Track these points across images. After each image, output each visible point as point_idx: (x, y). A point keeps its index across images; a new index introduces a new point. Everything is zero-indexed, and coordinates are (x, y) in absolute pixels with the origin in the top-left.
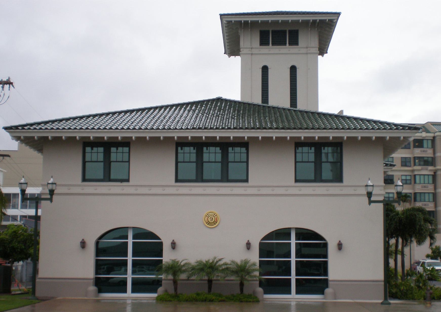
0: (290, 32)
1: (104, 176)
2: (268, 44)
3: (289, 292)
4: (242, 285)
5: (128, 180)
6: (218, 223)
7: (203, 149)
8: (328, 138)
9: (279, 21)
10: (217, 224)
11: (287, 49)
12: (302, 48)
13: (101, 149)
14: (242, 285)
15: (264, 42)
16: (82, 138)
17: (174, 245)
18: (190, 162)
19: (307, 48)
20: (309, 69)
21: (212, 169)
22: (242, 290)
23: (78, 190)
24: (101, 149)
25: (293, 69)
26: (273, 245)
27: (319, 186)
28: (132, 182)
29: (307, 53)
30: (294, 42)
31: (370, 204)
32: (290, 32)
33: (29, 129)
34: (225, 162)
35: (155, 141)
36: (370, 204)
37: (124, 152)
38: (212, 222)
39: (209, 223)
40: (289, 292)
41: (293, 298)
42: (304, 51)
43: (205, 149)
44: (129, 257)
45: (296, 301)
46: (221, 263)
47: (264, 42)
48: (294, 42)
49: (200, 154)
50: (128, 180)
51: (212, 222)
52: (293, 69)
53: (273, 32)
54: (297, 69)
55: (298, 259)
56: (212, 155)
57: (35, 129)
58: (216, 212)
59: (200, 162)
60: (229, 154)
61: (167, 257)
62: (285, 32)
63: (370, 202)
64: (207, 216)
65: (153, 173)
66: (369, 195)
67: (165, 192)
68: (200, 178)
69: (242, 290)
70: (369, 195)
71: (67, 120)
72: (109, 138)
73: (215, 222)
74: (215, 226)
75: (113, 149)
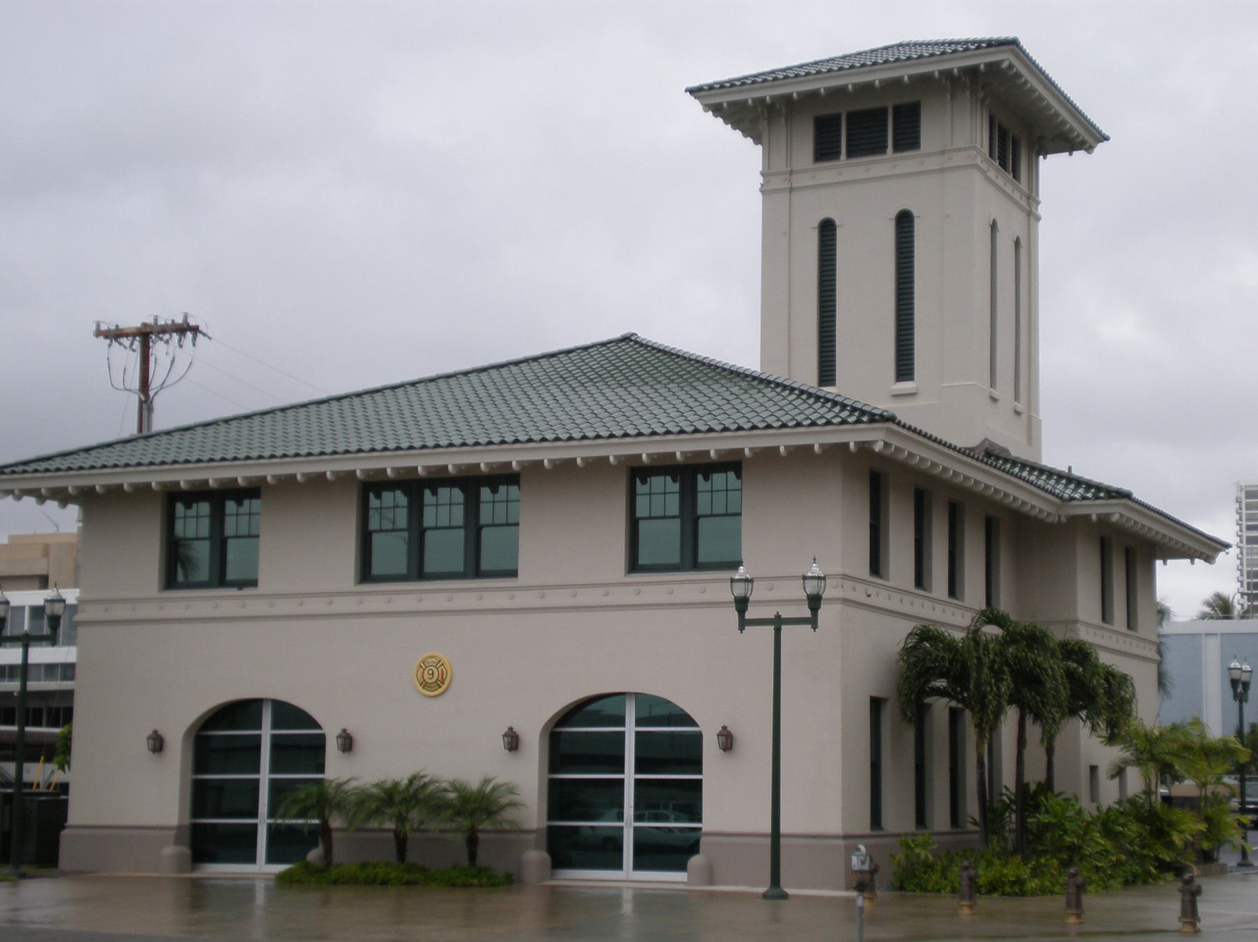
0: (898, 110)
1: (466, 566)
2: (879, 148)
3: (618, 865)
4: (472, 841)
5: (513, 574)
6: (446, 683)
7: (422, 495)
8: (206, 481)
9: (846, 86)
10: (444, 687)
11: (888, 164)
12: (930, 155)
13: (205, 508)
14: (472, 841)
15: (825, 151)
16: (164, 485)
17: (347, 743)
18: (665, 517)
19: (943, 153)
20: (948, 216)
21: (445, 546)
22: (473, 857)
23: (151, 611)
24: (205, 508)
25: (904, 221)
26: (577, 741)
27: (431, 591)
28: (263, 588)
29: (942, 171)
30: (908, 139)
31: (741, 628)
32: (898, 110)
33: (25, 472)
34: (690, 518)
35: (317, 482)
36: (741, 628)
37: (254, 510)
38: (435, 682)
39: (425, 685)
40: (618, 865)
41: (628, 877)
42: (933, 163)
43: (427, 493)
44: (248, 767)
45: (634, 889)
46: (354, 784)
47: (825, 151)
48: (908, 139)
49: (416, 509)
50: (513, 574)
51: (435, 682)
52: (904, 221)
53: (852, 117)
54: (916, 221)
55: (619, 776)
56: (444, 509)
57: (36, 471)
58: (441, 655)
59: (417, 534)
60: (482, 506)
61: (336, 768)
62: (883, 111)
63: (743, 623)
64: (423, 665)
65: (305, 560)
66: (742, 604)
67: (276, 611)
68: (418, 571)
69: (473, 857)
70: (742, 604)
71: (87, 450)
72: (221, 481)
73: (440, 682)
74: (440, 691)
75: (231, 506)
